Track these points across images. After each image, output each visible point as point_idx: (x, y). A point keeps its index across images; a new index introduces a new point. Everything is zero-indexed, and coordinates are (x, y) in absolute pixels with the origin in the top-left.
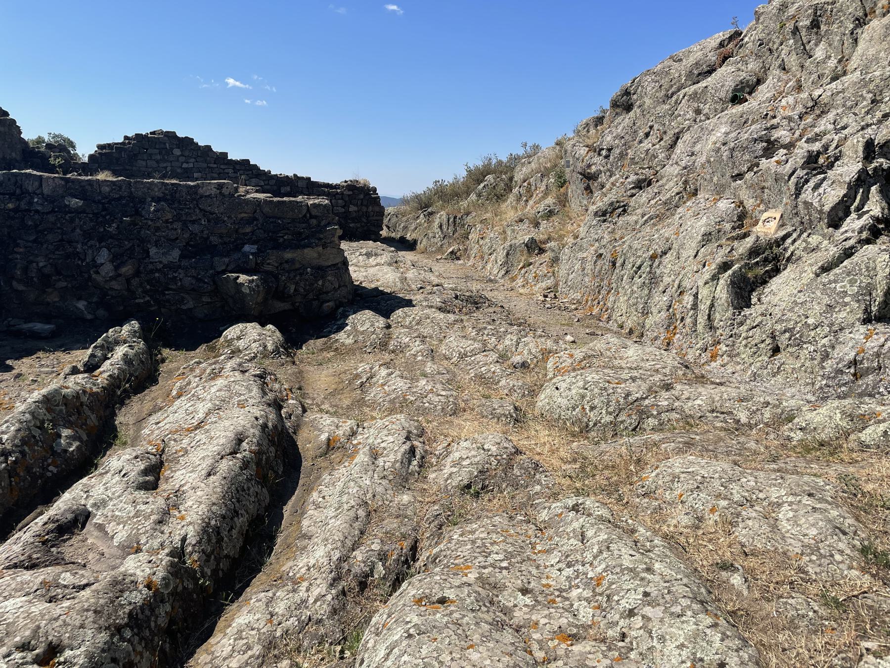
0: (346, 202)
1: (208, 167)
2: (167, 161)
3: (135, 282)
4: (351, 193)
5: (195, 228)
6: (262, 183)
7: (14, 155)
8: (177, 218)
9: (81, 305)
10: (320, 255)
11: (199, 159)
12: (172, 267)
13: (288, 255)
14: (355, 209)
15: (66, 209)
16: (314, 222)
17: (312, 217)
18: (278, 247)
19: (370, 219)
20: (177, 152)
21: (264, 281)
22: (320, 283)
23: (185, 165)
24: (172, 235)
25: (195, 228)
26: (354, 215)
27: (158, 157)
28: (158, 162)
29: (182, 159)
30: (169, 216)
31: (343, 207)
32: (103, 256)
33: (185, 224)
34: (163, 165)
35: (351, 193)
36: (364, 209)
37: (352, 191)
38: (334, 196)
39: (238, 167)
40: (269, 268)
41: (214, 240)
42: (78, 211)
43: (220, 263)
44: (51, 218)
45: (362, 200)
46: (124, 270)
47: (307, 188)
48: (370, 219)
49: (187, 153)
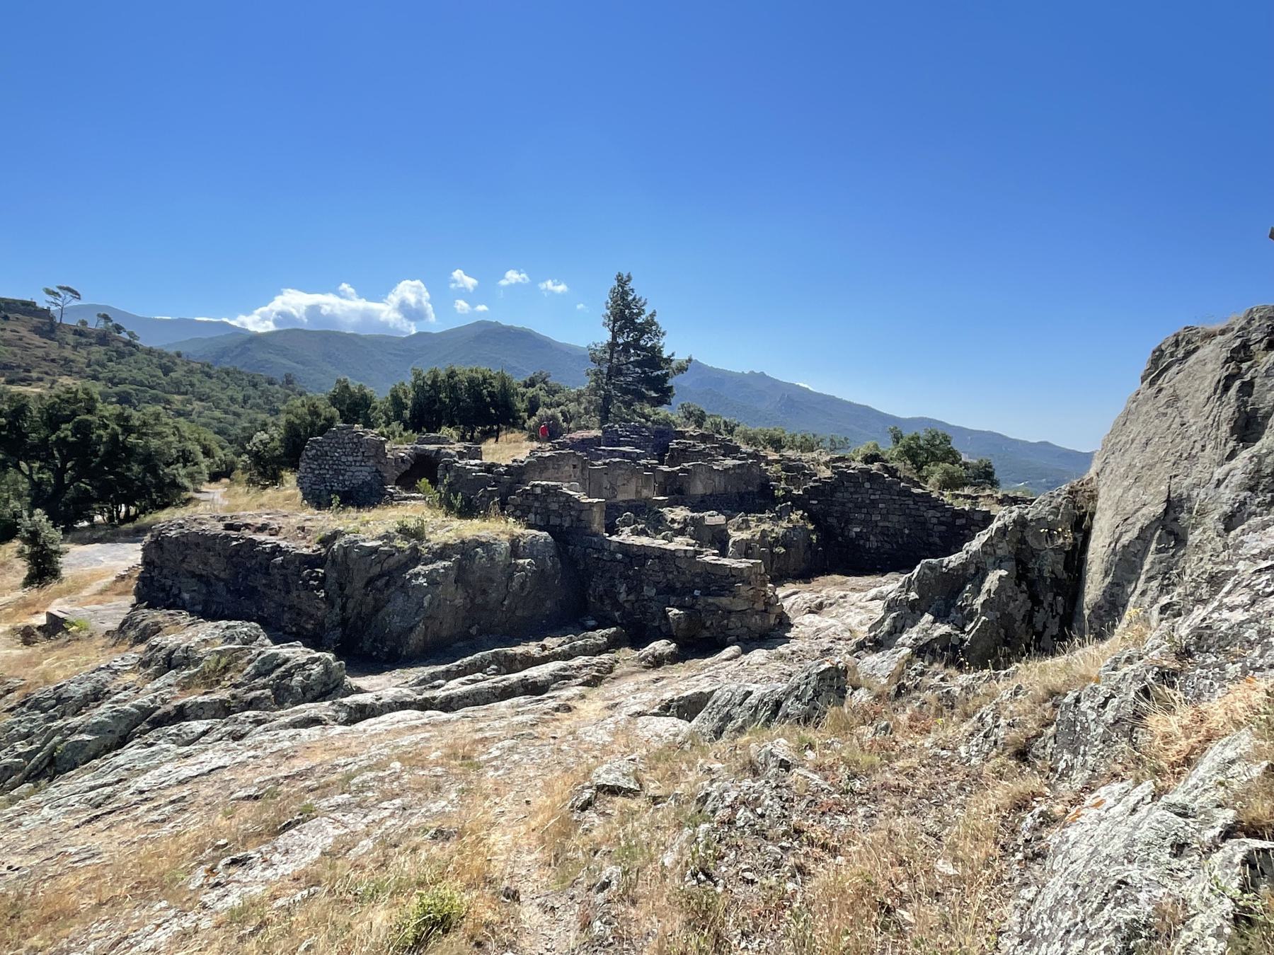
3: (636, 605)
5: (670, 576)
6: (939, 515)
7: (750, 488)
8: (663, 570)
9: (617, 614)
10: (732, 603)
11: (884, 491)
12: (651, 599)
13: (710, 600)
15: (614, 560)
16: (733, 579)
17: (733, 576)
18: (709, 594)
20: (867, 485)
21: (688, 616)
22: (725, 622)
23: (872, 497)
24: (657, 579)
25: (670, 576)
27: (852, 490)
28: (851, 493)
29: (870, 491)
30: (657, 568)
32: (623, 589)
33: (666, 575)
39: (917, 499)
40: (697, 607)
41: (678, 585)
42: (620, 561)
43: (672, 599)
44: (609, 564)
46: (630, 598)
49: (875, 486)
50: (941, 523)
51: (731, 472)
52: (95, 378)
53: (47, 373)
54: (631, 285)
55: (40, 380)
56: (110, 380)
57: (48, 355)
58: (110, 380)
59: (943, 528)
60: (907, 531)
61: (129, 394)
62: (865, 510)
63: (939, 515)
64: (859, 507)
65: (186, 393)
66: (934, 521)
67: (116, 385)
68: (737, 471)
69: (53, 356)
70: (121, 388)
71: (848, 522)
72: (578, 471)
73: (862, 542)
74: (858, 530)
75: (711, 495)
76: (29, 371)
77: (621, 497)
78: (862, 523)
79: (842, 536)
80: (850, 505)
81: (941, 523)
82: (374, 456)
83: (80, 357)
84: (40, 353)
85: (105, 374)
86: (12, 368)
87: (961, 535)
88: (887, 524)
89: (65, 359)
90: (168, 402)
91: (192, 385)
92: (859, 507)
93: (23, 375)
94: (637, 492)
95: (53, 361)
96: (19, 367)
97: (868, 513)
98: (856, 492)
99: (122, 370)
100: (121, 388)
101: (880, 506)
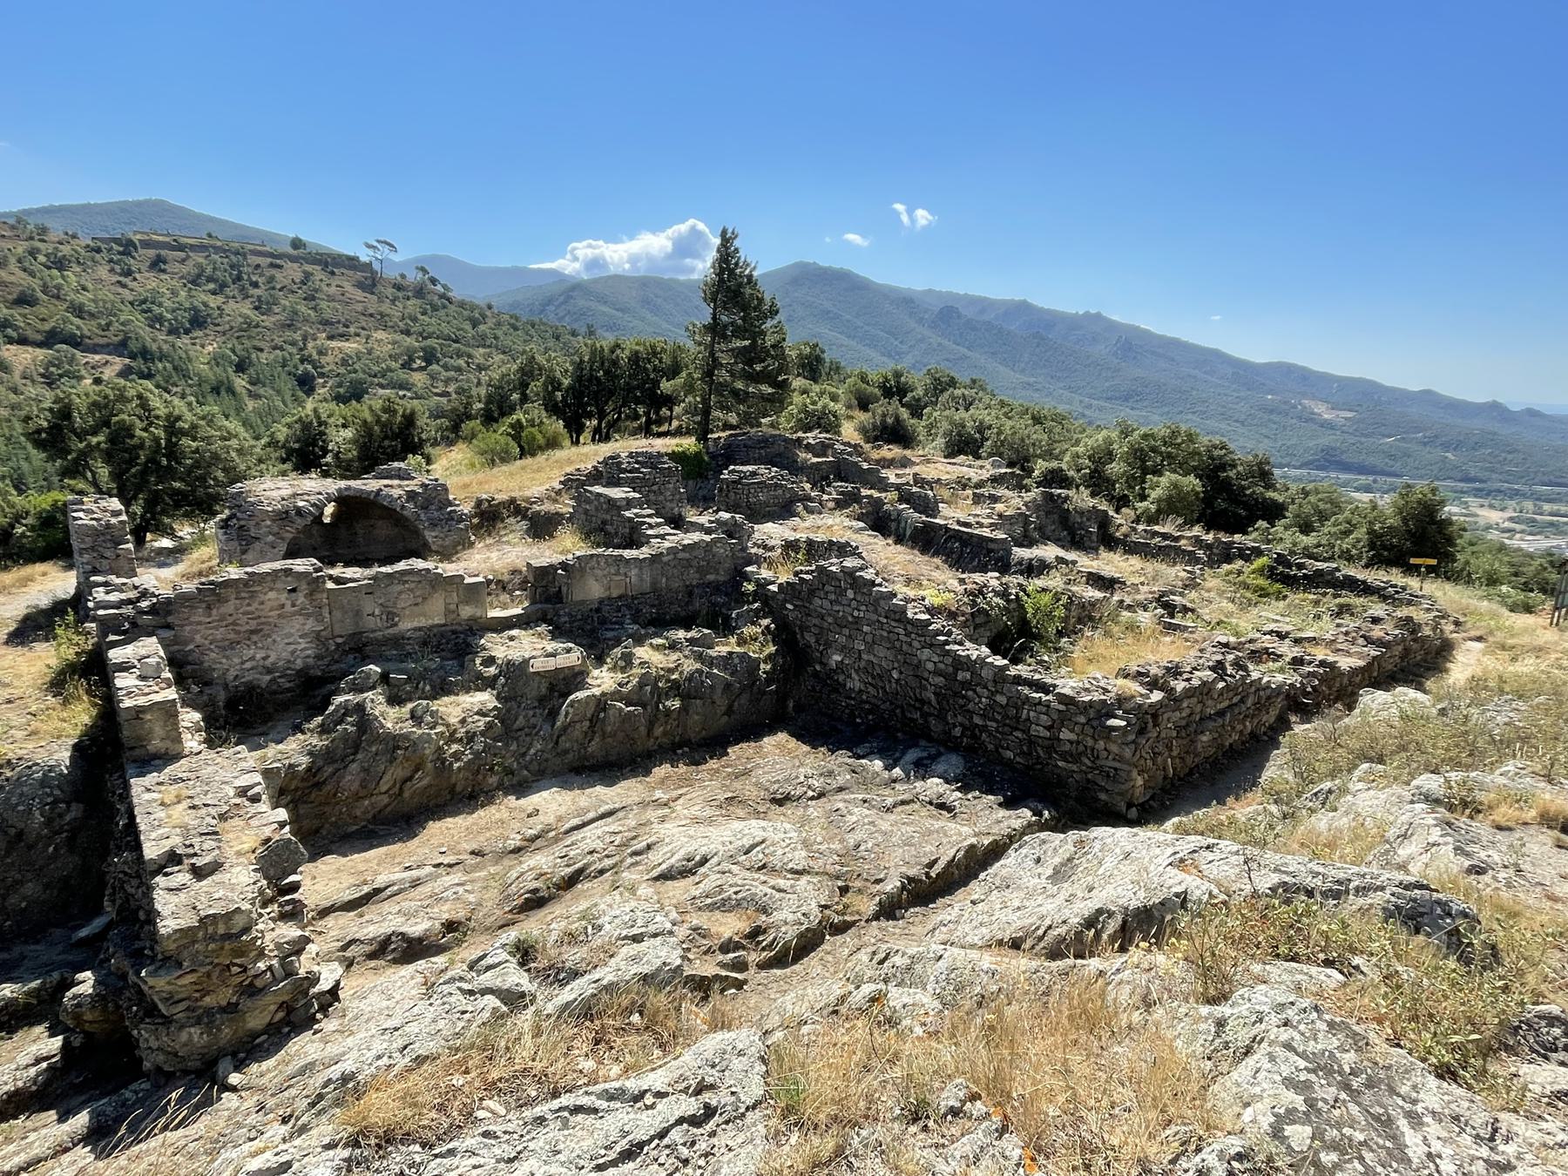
0: (1054, 721)
1: (878, 621)
2: (840, 604)
4: (1062, 707)
6: (936, 659)
14: (1073, 737)
19: (1098, 762)
20: (850, 594)
23: (856, 613)
26: (1067, 747)
27: (833, 597)
31: (1048, 728)
34: (836, 608)
35: (1062, 707)
36: (1090, 742)
37: (1066, 705)
38: (1035, 705)
45: (1084, 725)
47: (995, 681)
48: (1098, 762)
50: (937, 673)
51: (665, 559)
52: (407, 333)
53: (363, 329)
54: (737, 243)
55: (358, 335)
56: (421, 334)
57: (366, 309)
58: (421, 334)
59: (940, 680)
60: (895, 675)
61: (434, 348)
62: (846, 631)
63: (936, 659)
64: (840, 624)
65: (490, 347)
66: (930, 666)
67: (425, 338)
68: (681, 555)
69: (371, 311)
70: (429, 342)
71: (828, 645)
72: (301, 599)
73: (841, 678)
74: (839, 659)
75: (620, 597)
76: (348, 327)
77: (406, 625)
78: (842, 649)
79: (821, 663)
80: (830, 620)
81: (937, 673)
82: (93, 548)
83: (395, 312)
84: (359, 308)
85: (416, 328)
86: (332, 324)
87: (964, 697)
88: (872, 658)
89: (382, 315)
90: (470, 356)
91: (496, 338)
92: (840, 624)
93: (342, 329)
94: (448, 612)
95: (371, 315)
96: (339, 322)
97: (850, 636)
98: (837, 602)
99: (431, 322)
100: (429, 342)
101: (866, 629)
